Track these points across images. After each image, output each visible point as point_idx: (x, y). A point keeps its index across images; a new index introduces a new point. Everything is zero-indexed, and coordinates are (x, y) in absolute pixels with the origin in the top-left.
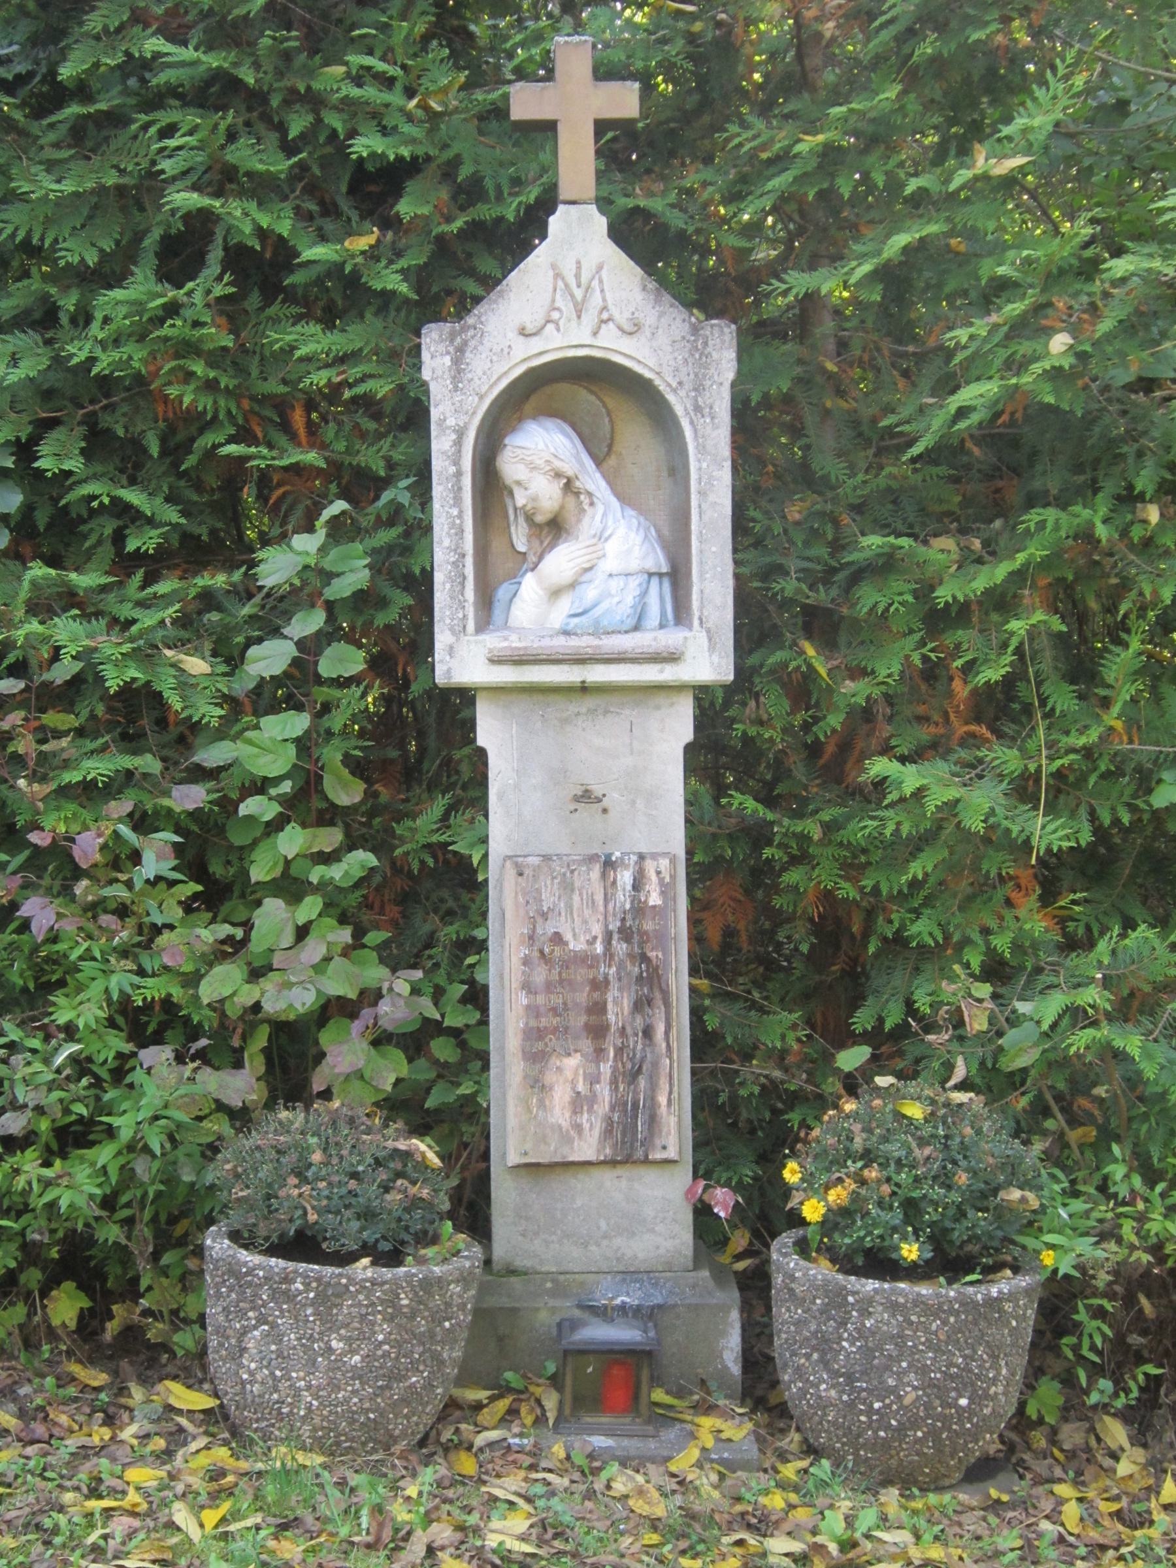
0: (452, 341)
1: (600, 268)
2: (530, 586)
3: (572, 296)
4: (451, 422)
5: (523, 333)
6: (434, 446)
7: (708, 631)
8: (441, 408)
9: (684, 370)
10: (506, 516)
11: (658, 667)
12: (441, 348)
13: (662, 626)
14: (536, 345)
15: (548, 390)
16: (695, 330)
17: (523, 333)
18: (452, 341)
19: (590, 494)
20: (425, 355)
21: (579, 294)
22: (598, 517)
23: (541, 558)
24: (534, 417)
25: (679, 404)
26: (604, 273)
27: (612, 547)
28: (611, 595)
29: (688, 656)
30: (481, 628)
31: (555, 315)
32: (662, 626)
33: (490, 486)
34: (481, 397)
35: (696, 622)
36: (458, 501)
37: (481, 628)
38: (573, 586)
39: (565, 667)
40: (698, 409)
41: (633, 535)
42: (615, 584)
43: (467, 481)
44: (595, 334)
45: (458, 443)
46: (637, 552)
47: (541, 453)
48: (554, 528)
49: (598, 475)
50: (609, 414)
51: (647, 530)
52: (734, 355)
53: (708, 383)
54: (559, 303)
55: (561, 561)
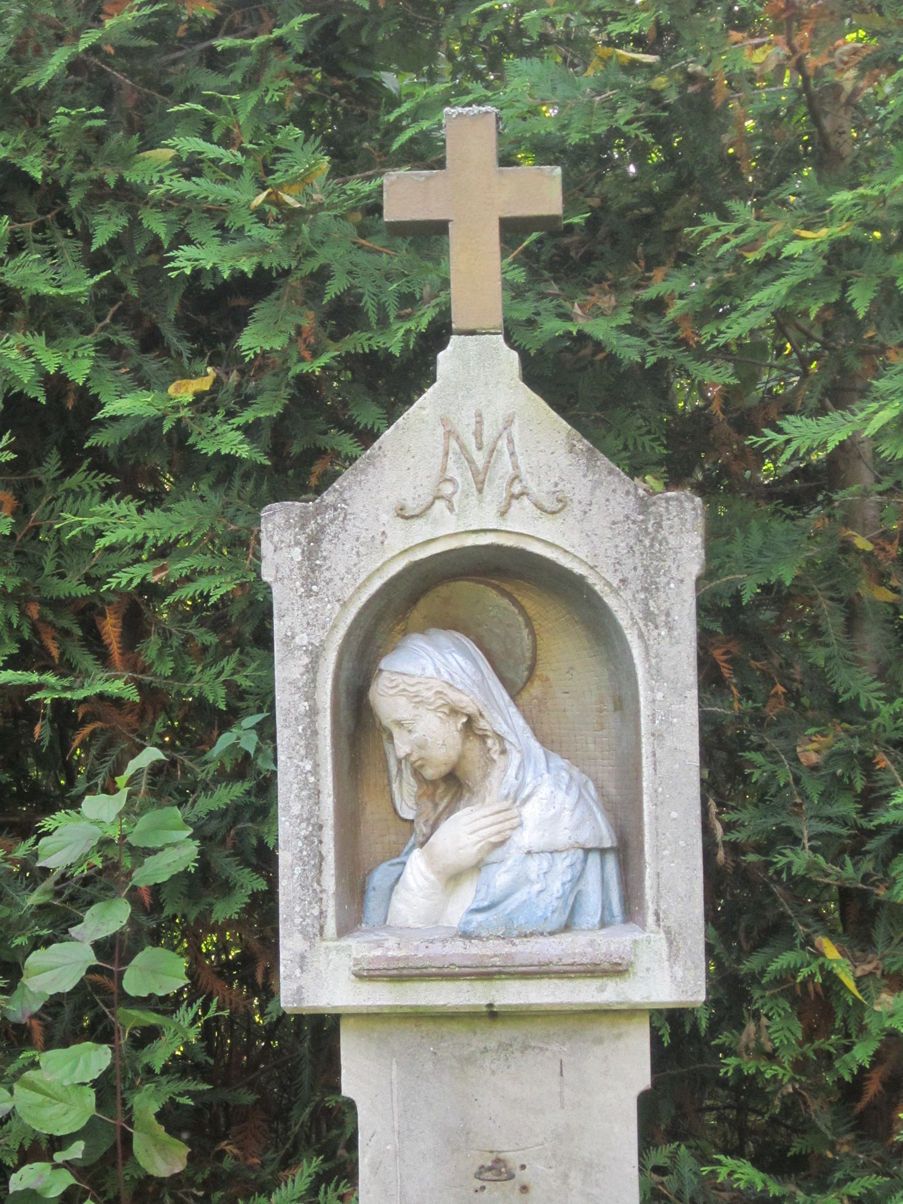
0: (303, 527)
1: (509, 422)
2: (417, 868)
3: (471, 461)
4: (302, 639)
5: (402, 514)
6: (280, 673)
7: (668, 932)
8: (288, 620)
9: (629, 562)
10: (387, 770)
11: (596, 983)
12: (289, 536)
13: (603, 924)
14: (421, 530)
15: (443, 591)
16: (644, 506)
17: (402, 514)
18: (303, 527)
19: (500, 738)
20: (266, 548)
21: (479, 458)
22: (512, 772)
23: (434, 827)
24: (422, 630)
25: (622, 610)
26: (515, 429)
27: (531, 812)
28: (528, 881)
29: (640, 967)
30: (344, 931)
31: (447, 489)
32: (603, 924)
34: (344, 605)
35: (651, 919)
36: (311, 750)
37: (344, 931)
38: (478, 866)
39: (464, 985)
40: (648, 616)
41: (561, 795)
42: (535, 866)
43: (325, 723)
44: (503, 514)
45: (312, 669)
46: (567, 819)
47: (432, 680)
48: (452, 786)
49: (513, 710)
50: (529, 622)
51: (583, 786)
52: (699, 540)
53: (663, 580)
54: (453, 472)
55: (461, 832)
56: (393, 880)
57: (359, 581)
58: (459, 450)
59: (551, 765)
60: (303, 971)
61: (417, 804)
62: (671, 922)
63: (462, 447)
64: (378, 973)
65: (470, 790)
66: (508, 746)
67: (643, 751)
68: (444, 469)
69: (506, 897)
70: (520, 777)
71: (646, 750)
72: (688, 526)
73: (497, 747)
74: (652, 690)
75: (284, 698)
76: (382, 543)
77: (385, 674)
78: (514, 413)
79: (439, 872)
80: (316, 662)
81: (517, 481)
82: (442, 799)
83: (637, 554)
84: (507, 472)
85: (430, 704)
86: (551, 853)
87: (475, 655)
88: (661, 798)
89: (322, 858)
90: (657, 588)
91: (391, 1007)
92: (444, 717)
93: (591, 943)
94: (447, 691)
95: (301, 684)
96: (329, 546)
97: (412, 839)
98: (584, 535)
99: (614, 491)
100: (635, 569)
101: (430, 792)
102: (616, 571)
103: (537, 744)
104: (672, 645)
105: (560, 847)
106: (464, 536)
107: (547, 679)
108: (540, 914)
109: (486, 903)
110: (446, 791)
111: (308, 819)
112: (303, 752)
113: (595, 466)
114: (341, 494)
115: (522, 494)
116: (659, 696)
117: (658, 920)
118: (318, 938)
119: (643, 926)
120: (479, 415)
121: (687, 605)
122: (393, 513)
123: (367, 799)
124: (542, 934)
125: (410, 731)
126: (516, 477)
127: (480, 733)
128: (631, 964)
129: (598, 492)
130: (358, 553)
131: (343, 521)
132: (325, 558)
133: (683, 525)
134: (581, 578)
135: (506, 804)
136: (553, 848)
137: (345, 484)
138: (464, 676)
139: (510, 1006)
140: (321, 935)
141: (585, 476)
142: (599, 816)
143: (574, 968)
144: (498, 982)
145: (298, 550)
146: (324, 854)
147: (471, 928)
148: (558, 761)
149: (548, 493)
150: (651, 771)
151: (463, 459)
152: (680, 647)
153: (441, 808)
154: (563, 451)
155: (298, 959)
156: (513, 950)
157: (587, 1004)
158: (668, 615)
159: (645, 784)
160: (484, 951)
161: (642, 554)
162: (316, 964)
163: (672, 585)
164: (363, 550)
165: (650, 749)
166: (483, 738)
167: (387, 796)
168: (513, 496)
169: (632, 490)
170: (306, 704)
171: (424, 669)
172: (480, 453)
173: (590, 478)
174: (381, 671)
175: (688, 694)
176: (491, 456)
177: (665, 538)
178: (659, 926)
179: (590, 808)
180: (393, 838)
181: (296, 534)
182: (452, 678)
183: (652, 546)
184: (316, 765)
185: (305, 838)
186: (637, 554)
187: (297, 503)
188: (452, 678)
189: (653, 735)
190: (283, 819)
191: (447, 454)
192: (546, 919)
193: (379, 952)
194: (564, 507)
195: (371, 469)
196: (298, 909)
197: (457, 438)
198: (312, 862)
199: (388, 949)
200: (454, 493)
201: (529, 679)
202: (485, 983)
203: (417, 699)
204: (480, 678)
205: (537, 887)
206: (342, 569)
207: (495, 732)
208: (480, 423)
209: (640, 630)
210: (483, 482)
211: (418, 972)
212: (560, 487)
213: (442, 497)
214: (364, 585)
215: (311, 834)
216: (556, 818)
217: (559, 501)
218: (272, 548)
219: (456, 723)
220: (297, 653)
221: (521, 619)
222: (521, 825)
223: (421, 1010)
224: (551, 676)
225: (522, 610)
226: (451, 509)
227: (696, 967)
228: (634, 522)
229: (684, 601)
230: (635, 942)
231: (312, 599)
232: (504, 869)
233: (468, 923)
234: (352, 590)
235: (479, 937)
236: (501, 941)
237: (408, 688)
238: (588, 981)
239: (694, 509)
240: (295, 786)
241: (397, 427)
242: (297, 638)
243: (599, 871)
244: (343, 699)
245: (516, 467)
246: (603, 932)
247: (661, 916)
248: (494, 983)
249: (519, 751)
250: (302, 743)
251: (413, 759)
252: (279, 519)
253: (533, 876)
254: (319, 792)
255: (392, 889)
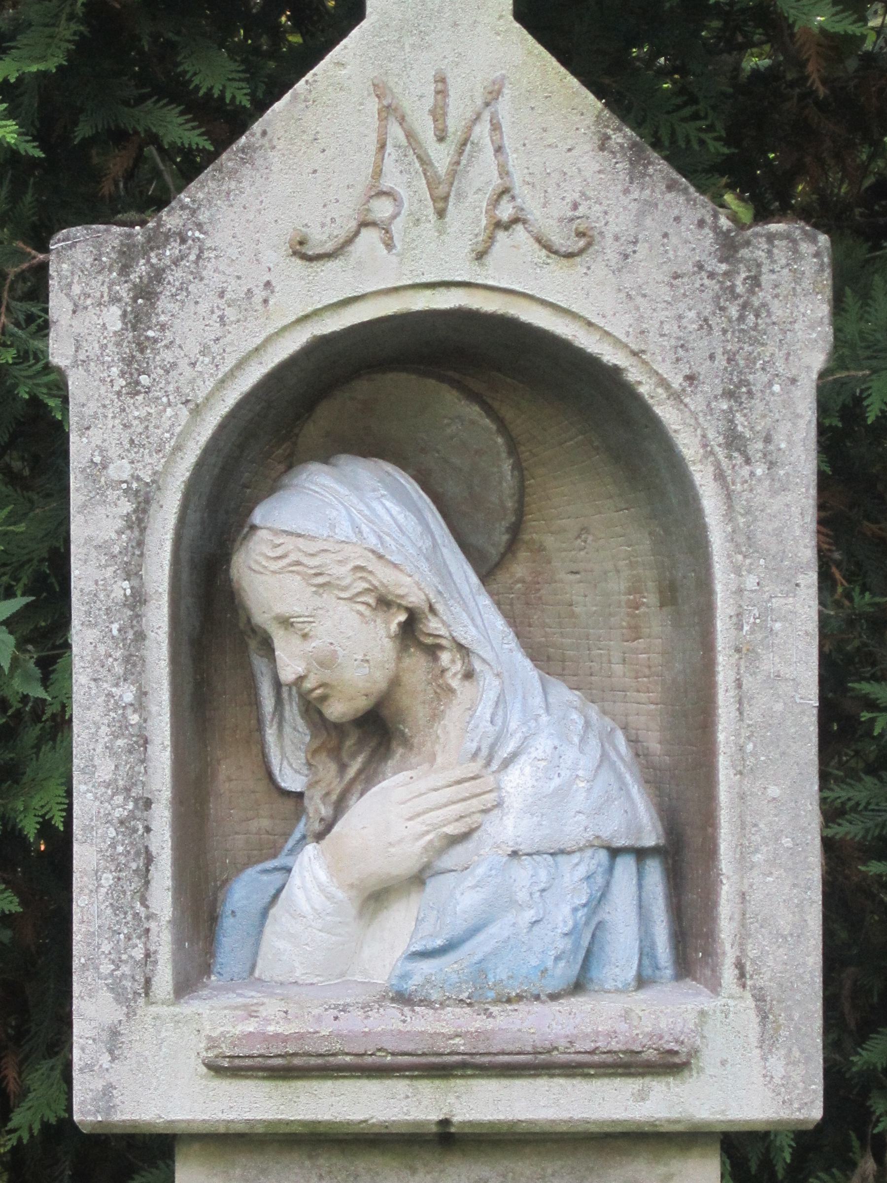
0: (125, 270)
1: (494, 94)
2: (313, 877)
3: (424, 161)
4: (120, 470)
5: (302, 252)
6: (79, 529)
7: (760, 998)
8: (96, 435)
9: (701, 346)
10: (255, 703)
11: (632, 1085)
12: (99, 286)
13: (641, 982)
14: (332, 281)
15: (363, 387)
16: (729, 247)
17: (302, 252)
18: (125, 270)
19: (462, 648)
20: (58, 305)
21: (441, 157)
22: (484, 710)
23: (340, 807)
24: (325, 457)
25: (688, 429)
26: (504, 107)
27: (517, 781)
28: (513, 903)
29: (709, 1059)
30: (186, 985)
31: (382, 209)
32: (641, 982)
33: (215, 630)
34: (197, 411)
35: (728, 974)
36: (133, 665)
37: (186, 985)
38: (419, 879)
39: (400, 1086)
40: (734, 441)
41: (570, 754)
42: (523, 875)
43: (158, 618)
44: (480, 256)
45: (138, 522)
46: (580, 798)
47: (343, 542)
48: (375, 733)
49: (485, 601)
50: (513, 448)
51: (606, 738)
52: (824, 310)
53: (759, 379)
54: (392, 180)
55: (391, 814)
56: (267, 899)
57: (225, 369)
58: (403, 141)
59: (550, 700)
60: (114, 1059)
61: (309, 765)
62: (763, 981)
63: (410, 135)
64: (248, 1062)
65: (406, 742)
66: (478, 666)
67: (720, 678)
68: (378, 173)
69: (474, 931)
70: (499, 721)
71: (724, 676)
72: (806, 284)
73: (458, 666)
74: (737, 570)
75: (84, 573)
76: (266, 301)
77: (262, 534)
78: (504, 77)
79: (352, 886)
80: (145, 511)
81: (506, 198)
82: (353, 756)
83: (717, 332)
84: (488, 183)
85: (345, 589)
86: (552, 854)
87: (420, 504)
88: (750, 761)
89: (149, 859)
90: (750, 393)
91: (270, 1123)
92: (367, 611)
93: (626, 1015)
94: (373, 564)
95: (116, 549)
96: (170, 306)
97: (302, 825)
98: (622, 295)
99: (677, 219)
100: (712, 357)
101: (333, 743)
102: (678, 360)
103: (528, 663)
104: (774, 493)
105: (569, 845)
106: (410, 293)
107: (541, 549)
108: (534, 962)
109: (439, 942)
110: (360, 744)
111: (127, 790)
112: (119, 669)
113: (644, 175)
114: (194, 212)
115: (516, 221)
116: (751, 582)
117: (742, 975)
118: (141, 1001)
119: (715, 987)
120: (441, 79)
121: (802, 424)
122: (285, 249)
123: (219, 753)
124: (537, 998)
125: (305, 636)
126: (506, 191)
127: (429, 641)
128: (695, 1052)
129: (648, 222)
130: (222, 318)
131: (196, 262)
132: (163, 327)
133: (797, 281)
134: (616, 371)
135: (475, 767)
136: (556, 847)
137: (200, 195)
138: (403, 540)
139: (480, 1124)
140: (147, 994)
141: (626, 191)
142: (635, 790)
143: (596, 1058)
144: (459, 1082)
145: (116, 310)
146: (153, 850)
147: (410, 986)
148: (561, 693)
149: (561, 220)
150: (734, 714)
151: (412, 157)
152: (789, 498)
153: (352, 772)
154: (588, 147)
155: (105, 1036)
156: (490, 1025)
157: (614, 1122)
158: (768, 440)
159: (721, 737)
160: (438, 1027)
161: (725, 332)
162: (136, 1045)
163: (776, 388)
164: (231, 314)
165: (732, 675)
166: (432, 650)
167: (255, 749)
168: (499, 225)
169: (709, 219)
170: (126, 584)
171: (333, 527)
172: (443, 146)
173: (636, 195)
174: (254, 528)
175: (802, 579)
176: (461, 154)
177: (764, 305)
178: (744, 986)
179: (620, 778)
180: (265, 823)
181: (112, 283)
182: (382, 543)
183: (742, 318)
184: (142, 694)
185: (122, 822)
186: (717, 332)
187: (115, 229)
188: (382, 543)
189: (738, 650)
190: (83, 788)
191: (382, 146)
192: (544, 971)
193: (251, 1027)
194: (589, 245)
195: (246, 170)
196: (106, 947)
197: (402, 120)
198: (134, 866)
199: (268, 1021)
200: (394, 217)
201: (511, 547)
202: (437, 1082)
203: (320, 580)
204: (429, 543)
205: (529, 915)
206: (192, 348)
207: (454, 639)
208: (442, 93)
209: (718, 465)
210: (446, 199)
211: (320, 1061)
212: (581, 210)
213: (374, 224)
214: (231, 375)
215: (132, 816)
216: (561, 794)
217: (581, 234)
218: (70, 306)
219: (387, 623)
220: (112, 495)
221: (500, 440)
222: (499, 805)
223: (322, 1129)
224: (550, 541)
225: (503, 427)
226: (389, 245)
227: (808, 1060)
228: (712, 275)
229: (799, 416)
230: (702, 1013)
231: (140, 398)
232: (470, 881)
233: (405, 976)
234: (210, 384)
235: (426, 1002)
236: (467, 1010)
237: (305, 560)
238: (618, 1082)
239: (817, 255)
240: (104, 730)
241: (295, 97)
242: (111, 466)
243: (634, 889)
244: (185, 576)
245: (504, 172)
246: (641, 995)
247: (748, 968)
248: (453, 1082)
249: (498, 675)
250: (118, 654)
251: (308, 685)
252: (82, 254)
253: (522, 896)
254: (146, 742)
255: (264, 913)
